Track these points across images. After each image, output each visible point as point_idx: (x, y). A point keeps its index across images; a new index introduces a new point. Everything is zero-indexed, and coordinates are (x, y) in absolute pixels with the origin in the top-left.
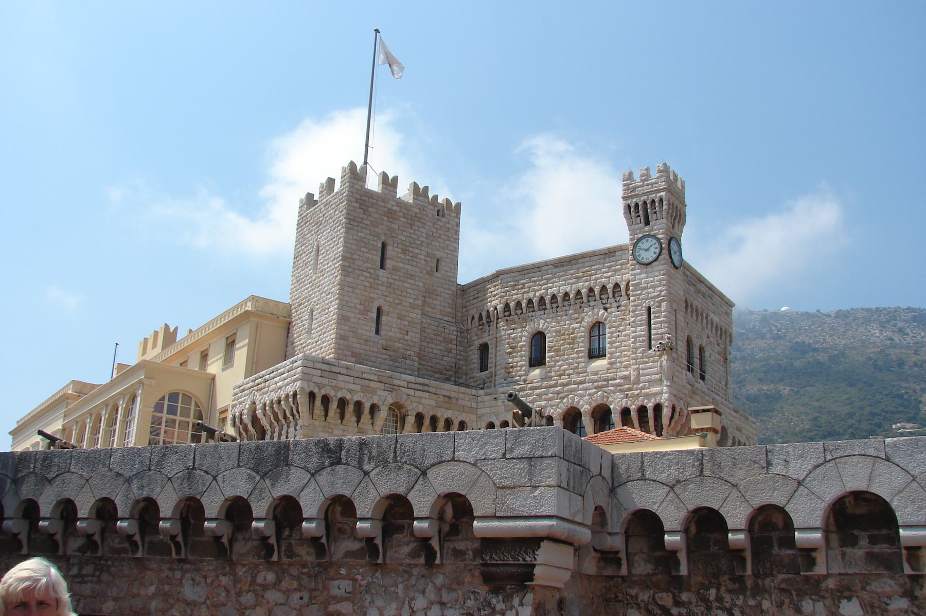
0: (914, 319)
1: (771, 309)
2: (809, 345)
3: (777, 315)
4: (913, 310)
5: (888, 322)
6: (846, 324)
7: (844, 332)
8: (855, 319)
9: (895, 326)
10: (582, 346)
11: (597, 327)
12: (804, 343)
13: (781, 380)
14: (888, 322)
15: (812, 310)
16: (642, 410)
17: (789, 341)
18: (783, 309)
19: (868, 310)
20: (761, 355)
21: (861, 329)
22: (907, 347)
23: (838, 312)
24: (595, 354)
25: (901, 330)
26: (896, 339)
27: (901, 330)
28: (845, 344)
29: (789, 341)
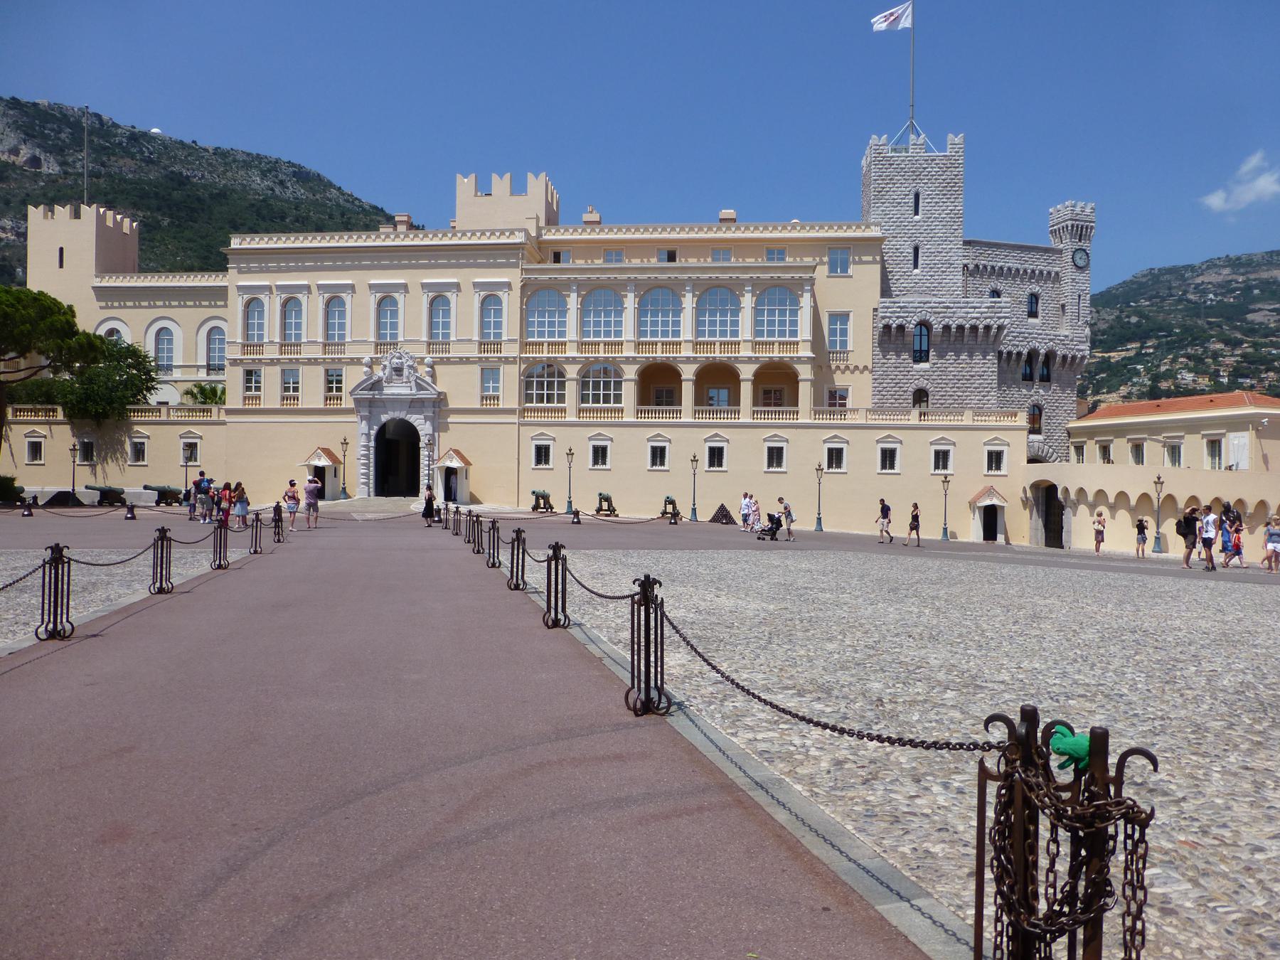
0: (295, 174)
1: (140, 128)
2: (188, 177)
3: (146, 136)
4: (294, 165)
5: (269, 171)
6: (226, 164)
7: (224, 173)
8: (235, 161)
9: (276, 177)
10: (1025, 308)
11: (1034, 298)
12: (181, 173)
13: (159, 209)
14: (269, 171)
15: (188, 140)
16: (1074, 357)
17: (164, 168)
18: (155, 130)
19: (248, 154)
20: (130, 176)
21: (242, 173)
22: (287, 201)
23: (216, 149)
24: (1033, 314)
25: (282, 183)
26: (278, 190)
27: (282, 183)
28: (225, 185)
29: (164, 168)
